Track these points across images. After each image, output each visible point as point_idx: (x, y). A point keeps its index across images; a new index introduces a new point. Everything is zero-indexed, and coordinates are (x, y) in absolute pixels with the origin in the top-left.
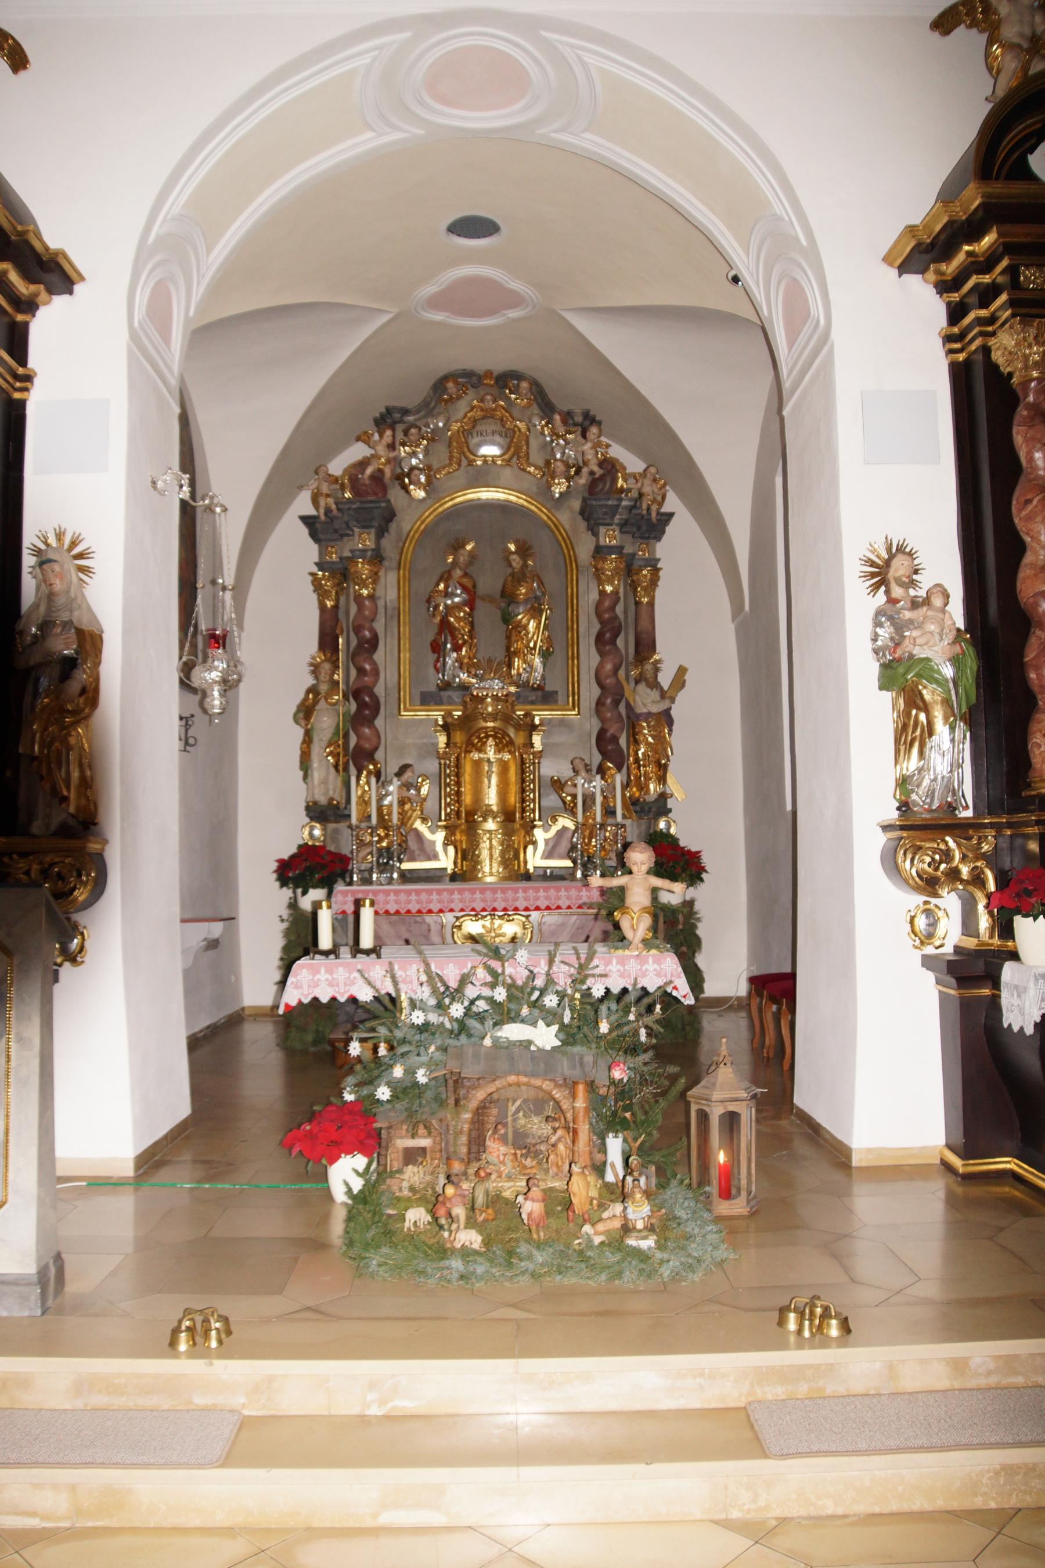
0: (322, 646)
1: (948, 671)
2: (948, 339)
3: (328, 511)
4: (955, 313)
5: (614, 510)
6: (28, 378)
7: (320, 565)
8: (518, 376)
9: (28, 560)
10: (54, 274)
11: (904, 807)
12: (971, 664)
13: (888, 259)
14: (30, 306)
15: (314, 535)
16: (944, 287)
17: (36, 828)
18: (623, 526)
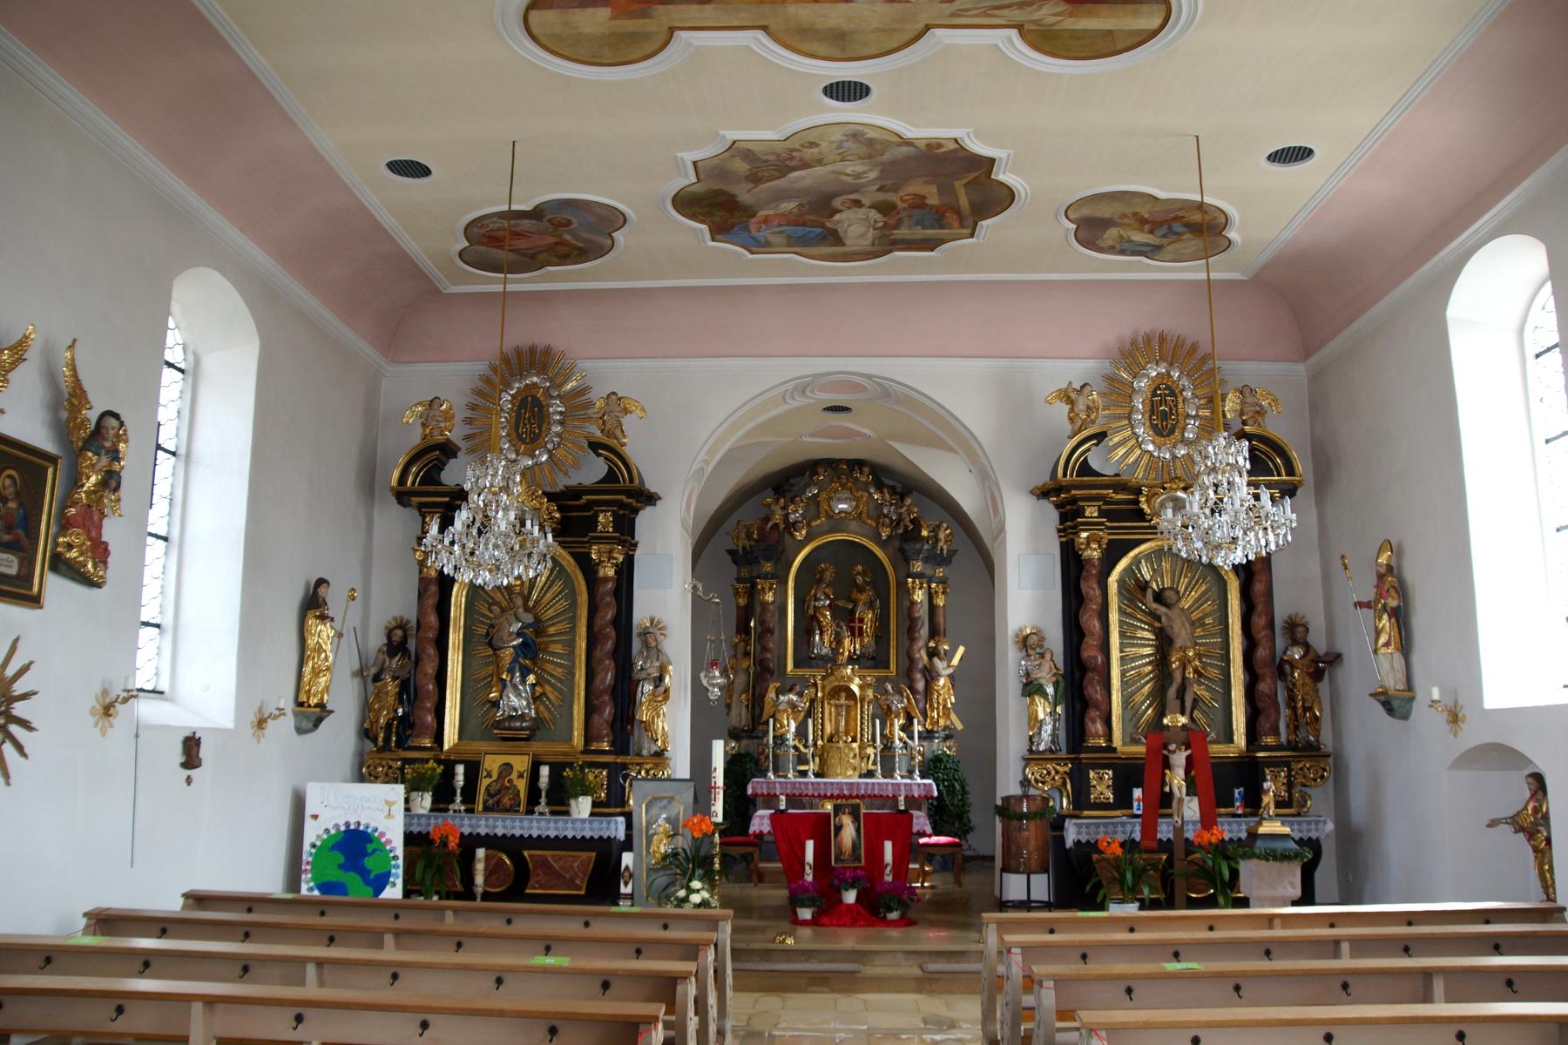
0: (738, 632)
1: (1050, 690)
2: (1059, 531)
3: (744, 548)
4: (1063, 518)
5: (920, 551)
6: (636, 545)
7: (739, 580)
8: (858, 464)
9: (635, 631)
10: (651, 499)
11: (1030, 751)
12: (1062, 685)
13: (1032, 492)
14: (636, 511)
15: (735, 561)
16: (1057, 506)
17: (645, 752)
18: (926, 560)
